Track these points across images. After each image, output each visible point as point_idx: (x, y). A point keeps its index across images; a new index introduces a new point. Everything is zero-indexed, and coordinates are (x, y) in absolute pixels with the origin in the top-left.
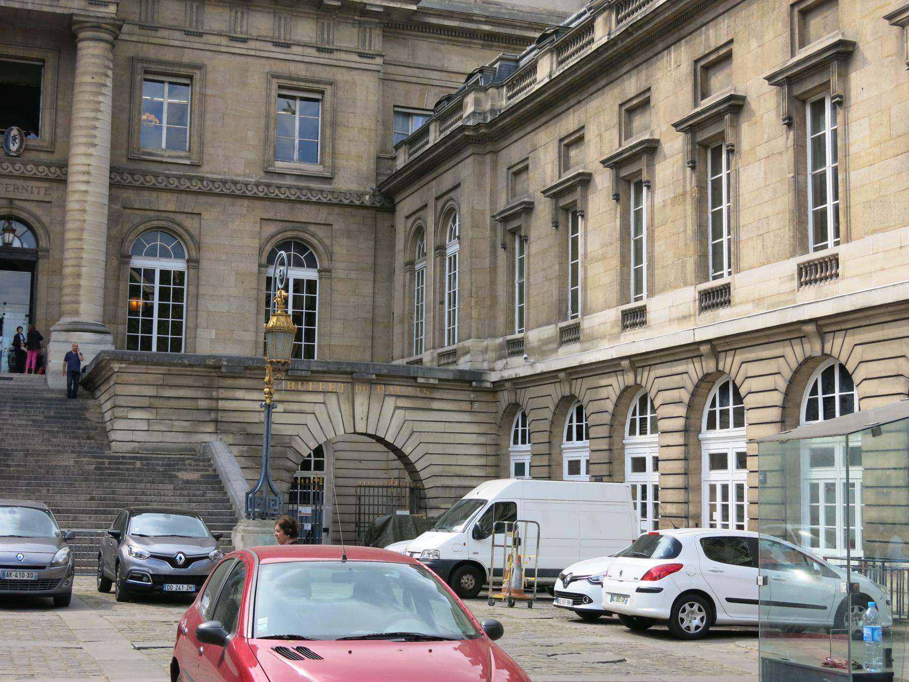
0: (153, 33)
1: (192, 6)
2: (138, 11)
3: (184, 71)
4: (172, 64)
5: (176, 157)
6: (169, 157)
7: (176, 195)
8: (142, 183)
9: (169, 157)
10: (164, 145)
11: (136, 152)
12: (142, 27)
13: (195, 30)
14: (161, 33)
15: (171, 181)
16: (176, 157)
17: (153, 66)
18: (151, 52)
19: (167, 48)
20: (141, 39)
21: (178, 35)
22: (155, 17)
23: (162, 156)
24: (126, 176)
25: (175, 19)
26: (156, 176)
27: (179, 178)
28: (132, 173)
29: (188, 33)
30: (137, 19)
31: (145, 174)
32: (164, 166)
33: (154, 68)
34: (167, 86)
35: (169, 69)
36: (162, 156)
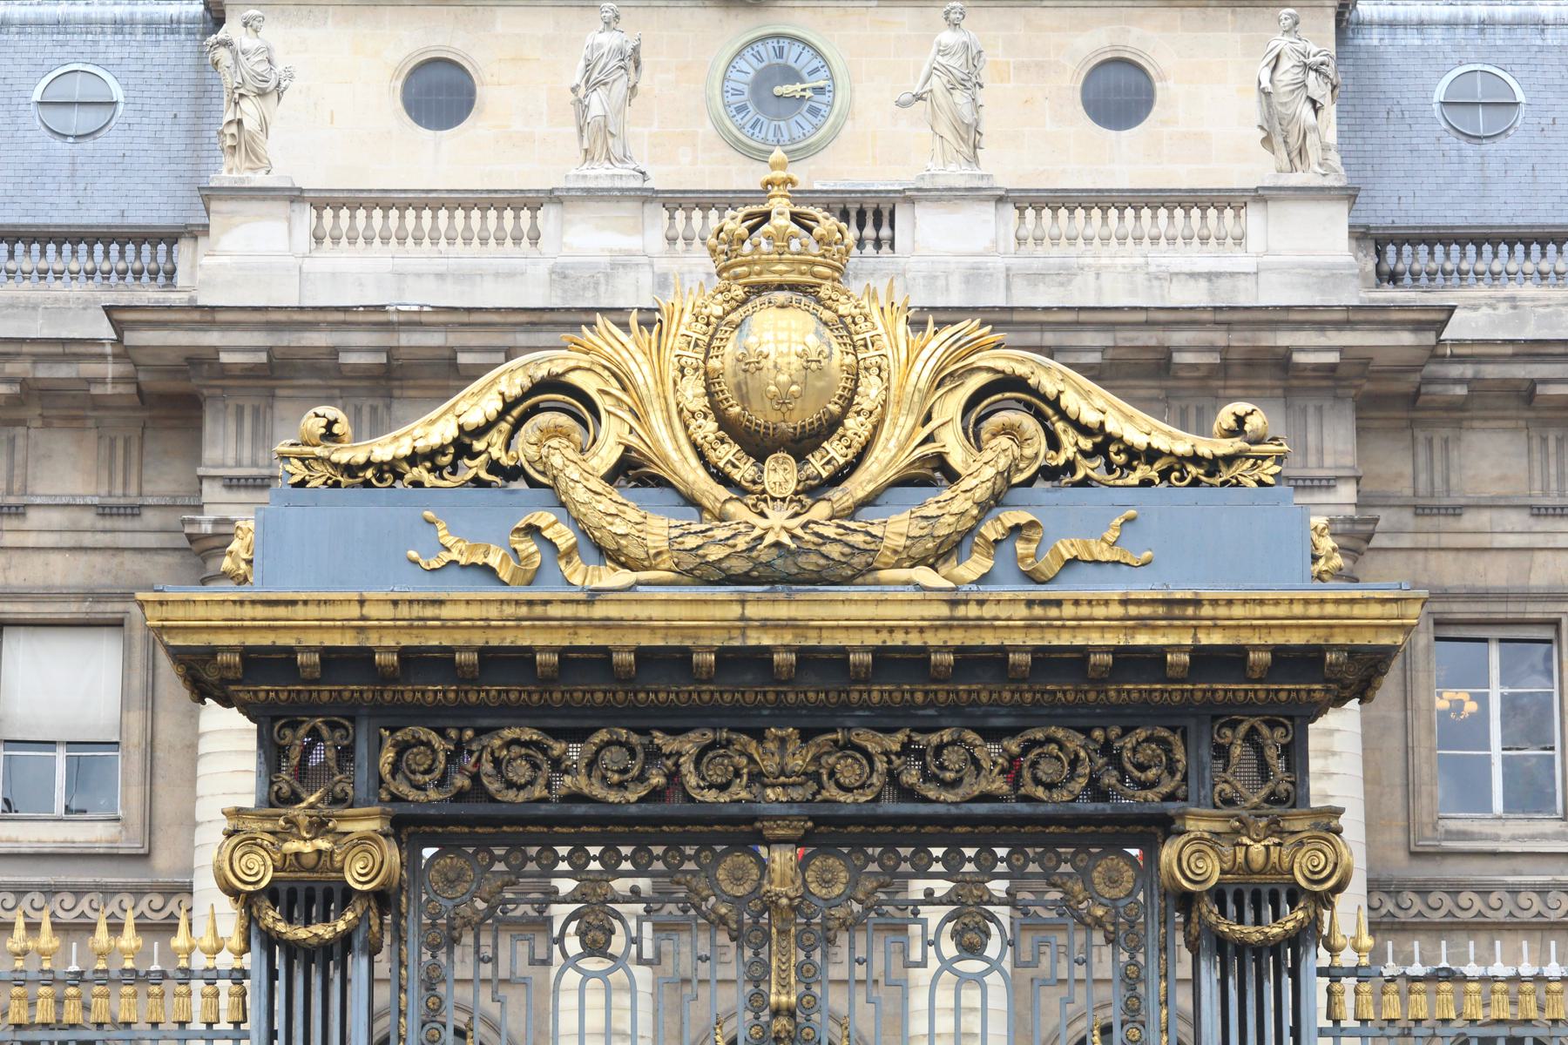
0: (1451, 523)
1: (1544, 440)
2: (1408, 470)
3: (1535, 611)
4: (1504, 596)
5: (1533, 837)
6: (1514, 838)
7: (1538, 935)
8: (1450, 914)
9: (1514, 838)
10: (1498, 805)
11: (1428, 832)
12: (1420, 510)
13: (1558, 502)
14: (1469, 520)
15: (1523, 900)
16: (1533, 837)
17: (1455, 607)
18: (1451, 572)
19: (1487, 557)
20: (1422, 540)
21: (1516, 519)
22: (1454, 480)
23: (1496, 838)
24: (1408, 898)
25: (1503, 478)
26: (1484, 891)
27: (1542, 891)
28: (1423, 890)
29: (1538, 512)
30: (1408, 492)
31: (1454, 890)
32: (1503, 864)
33: (1460, 610)
34: (1494, 651)
35: (1499, 610)
36: (1496, 838)
